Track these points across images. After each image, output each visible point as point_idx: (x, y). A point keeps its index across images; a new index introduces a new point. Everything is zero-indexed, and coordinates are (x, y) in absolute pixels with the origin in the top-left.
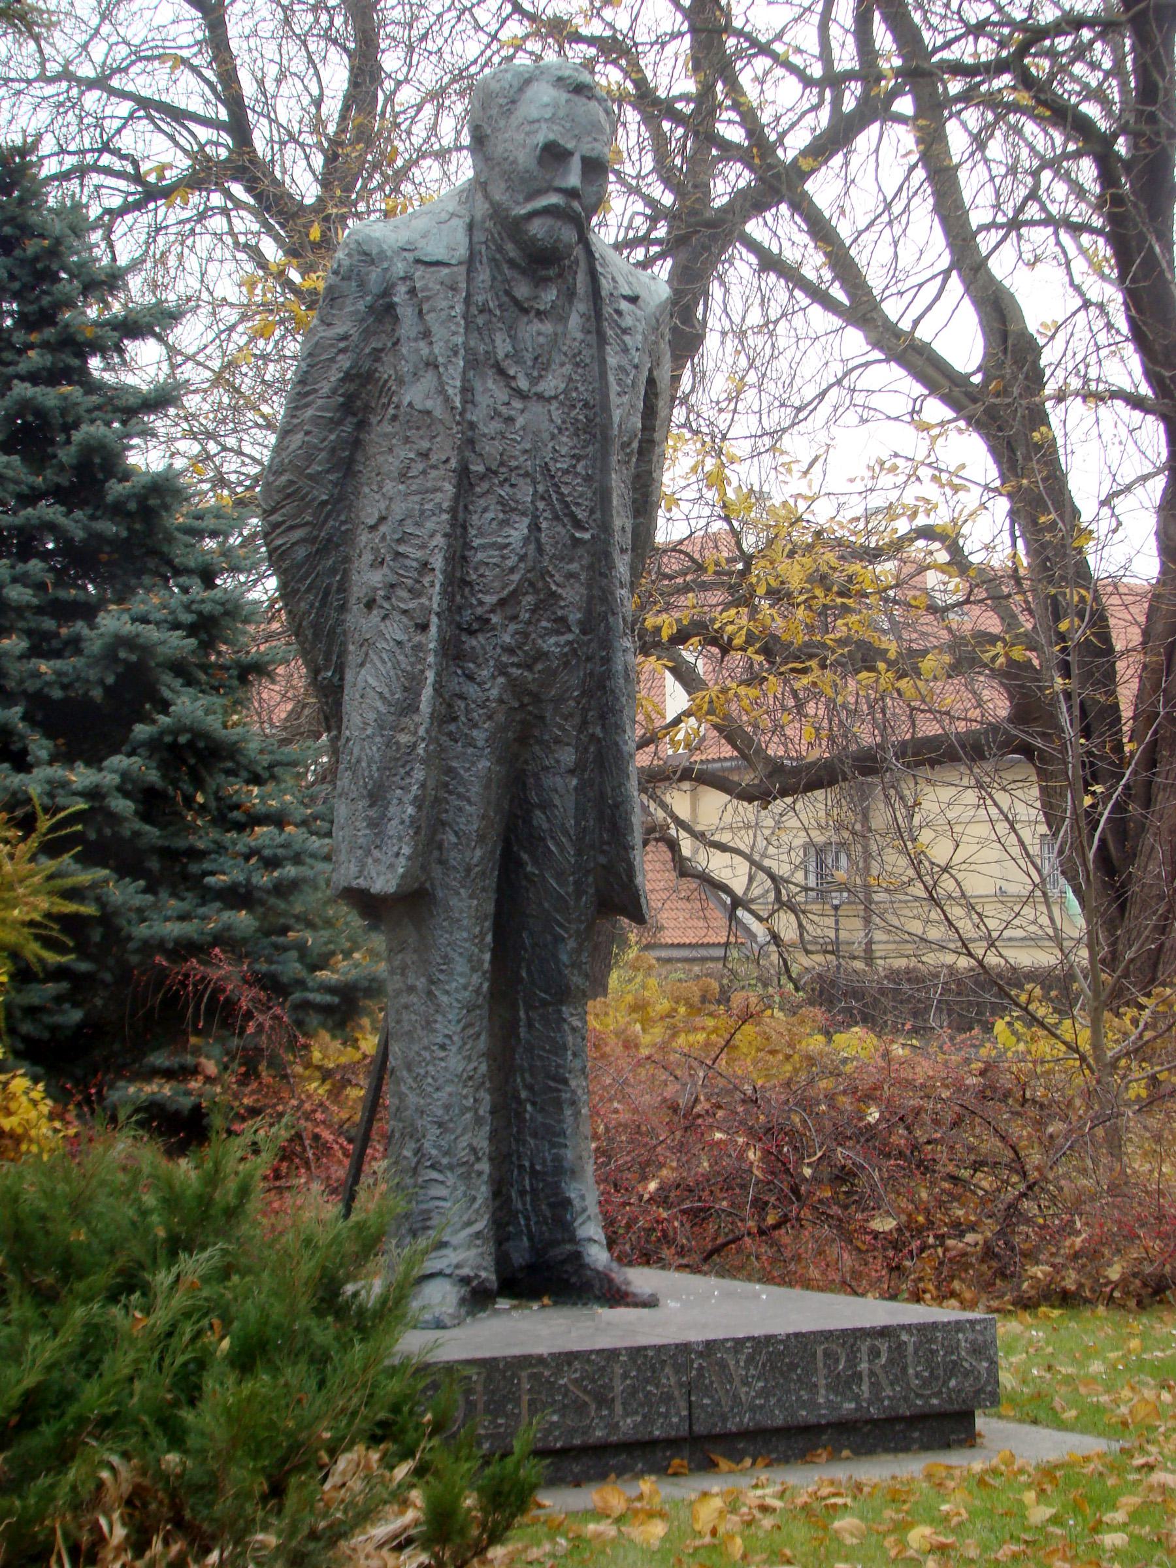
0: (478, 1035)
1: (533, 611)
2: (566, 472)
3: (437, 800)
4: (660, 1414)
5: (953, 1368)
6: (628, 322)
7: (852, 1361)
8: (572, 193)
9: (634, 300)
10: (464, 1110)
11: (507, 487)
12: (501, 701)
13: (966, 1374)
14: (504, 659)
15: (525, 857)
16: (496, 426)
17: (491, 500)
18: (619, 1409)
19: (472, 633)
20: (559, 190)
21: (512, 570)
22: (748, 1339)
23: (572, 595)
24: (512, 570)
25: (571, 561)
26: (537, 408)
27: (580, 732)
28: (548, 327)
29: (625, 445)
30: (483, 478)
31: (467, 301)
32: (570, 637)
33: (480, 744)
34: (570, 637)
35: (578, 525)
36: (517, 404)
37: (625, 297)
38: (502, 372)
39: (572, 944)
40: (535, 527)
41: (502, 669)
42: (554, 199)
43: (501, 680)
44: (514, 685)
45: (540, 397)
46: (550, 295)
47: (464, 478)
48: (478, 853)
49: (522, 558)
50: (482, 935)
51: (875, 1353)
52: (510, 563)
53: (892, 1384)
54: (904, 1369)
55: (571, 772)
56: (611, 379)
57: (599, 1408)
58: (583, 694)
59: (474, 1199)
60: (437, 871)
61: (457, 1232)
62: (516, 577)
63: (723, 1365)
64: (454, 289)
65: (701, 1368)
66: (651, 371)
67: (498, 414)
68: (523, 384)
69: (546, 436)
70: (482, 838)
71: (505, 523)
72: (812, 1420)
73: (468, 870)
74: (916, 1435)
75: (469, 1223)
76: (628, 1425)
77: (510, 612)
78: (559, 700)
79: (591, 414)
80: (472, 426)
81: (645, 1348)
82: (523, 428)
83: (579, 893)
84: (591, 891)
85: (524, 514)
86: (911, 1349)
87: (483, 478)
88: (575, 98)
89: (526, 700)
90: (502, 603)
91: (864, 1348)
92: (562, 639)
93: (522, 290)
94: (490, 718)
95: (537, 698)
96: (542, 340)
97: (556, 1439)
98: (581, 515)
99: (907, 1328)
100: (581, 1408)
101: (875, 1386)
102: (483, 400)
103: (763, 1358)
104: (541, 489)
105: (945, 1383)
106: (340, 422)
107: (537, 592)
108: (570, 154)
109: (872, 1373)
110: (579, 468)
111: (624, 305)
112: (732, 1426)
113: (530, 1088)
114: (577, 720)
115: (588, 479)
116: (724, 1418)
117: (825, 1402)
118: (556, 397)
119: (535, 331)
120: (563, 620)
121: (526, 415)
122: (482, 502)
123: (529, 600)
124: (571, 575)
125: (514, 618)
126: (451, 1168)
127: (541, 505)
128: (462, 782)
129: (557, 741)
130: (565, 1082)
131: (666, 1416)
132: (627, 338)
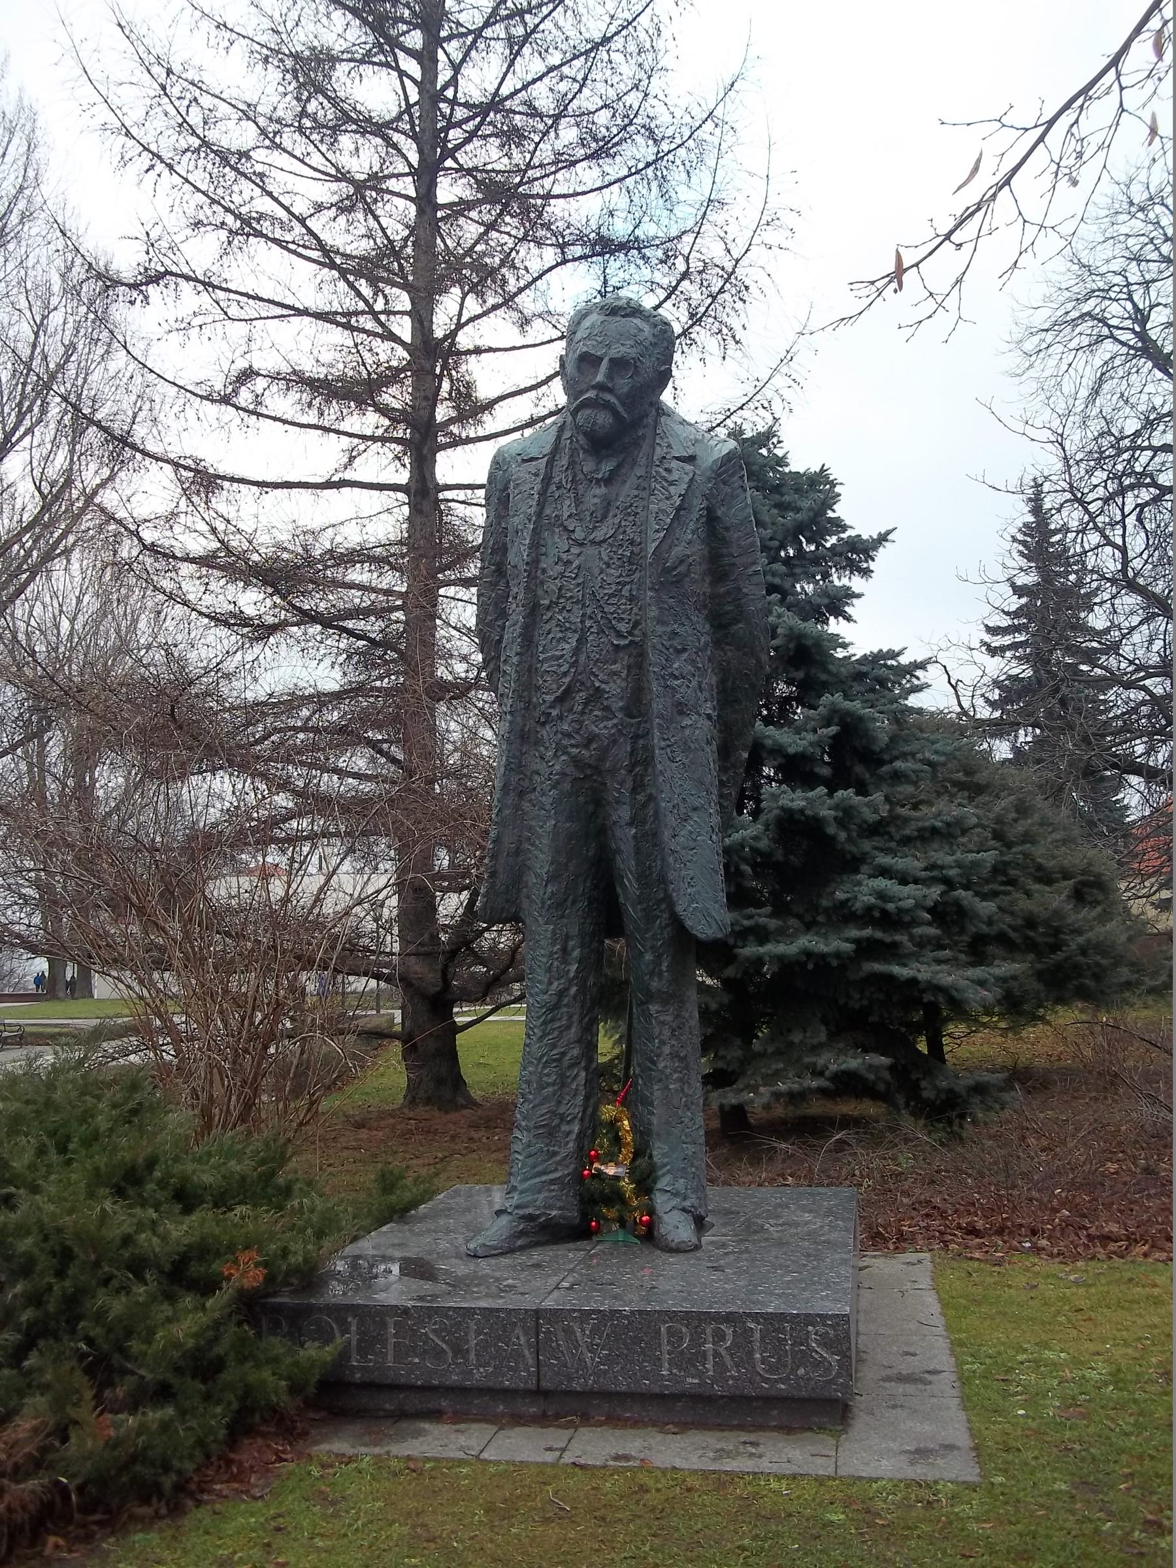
0: (569, 1027)
1: (586, 704)
2: (611, 596)
3: (518, 852)
4: (510, 1368)
5: (804, 1358)
6: (675, 476)
7: (697, 1340)
8: (601, 387)
9: (691, 459)
10: (541, 1087)
11: (565, 614)
12: (563, 774)
13: (817, 1365)
14: (565, 742)
15: (619, 890)
16: (560, 568)
17: (554, 622)
18: (472, 1356)
19: (543, 724)
20: (594, 387)
21: (565, 674)
22: (593, 1311)
23: (614, 688)
24: (565, 674)
25: (615, 663)
26: (591, 551)
27: (634, 791)
28: (601, 491)
29: (667, 571)
30: (549, 608)
31: (547, 480)
32: (615, 721)
33: (548, 807)
34: (615, 721)
35: (619, 635)
36: (575, 550)
37: (677, 458)
38: (566, 529)
39: (648, 957)
40: (581, 641)
41: (560, 749)
42: (591, 394)
43: (563, 758)
44: (576, 762)
45: (593, 542)
46: (607, 467)
47: (533, 611)
48: (549, 890)
49: (572, 665)
50: (565, 951)
51: (719, 1336)
52: (564, 669)
53: (737, 1366)
54: (751, 1353)
55: (630, 824)
56: (652, 519)
57: (455, 1356)
58: (633, 765)
59: (555, 1154)
60: (525, 904)
61: (526, 1180)
62: (567, 680)
63: (569, 1331)
64: (536, 475)
65: (548, 1332)
66: (710, 510)
67: (559, 559)
68: (579, 535)
69: (596, 571)
70: (553, 878)
71: (563, 639)
72: (656, 1390)
73: (543, 903)
74: (775, 1412)
75: (544, 1173)
76: (480, 1376)
77: (567, 705)
78: (613, 771)
79: (636, 550)
80: (544, 571)
81: (498, 1310)
82: (579, 567)
83: (649, 918)
84: (666, 915)
85: (575, 631)
86: (757, 1335)
87: (549, 608)
88: (610, 318)
89: (589, 772)
90: (560, 700)
91: (708, 1331)
92: (610, 724)
93: (588, 466)
94: (553, 787)
95: (597, 770)
96: (596, 500)
97: (417, 1378)
98: (623, 627)
99: (755, 1317)
100: (439, 1354)
101: (720, 1366)
102: (552, 552)
103: (608, 1330)
104: (589, 611)
105: (794, 1370)
106: (497, 584)
107: (587, 689)
108: (600, 359)
109: (716, 1354)
110: (625, 592)
111: (675, 464)
112: (576, 1386)
113: (639, 1065)
114: (629, 784)
115: (632, 598)
116: (570, 1379)
117: (667, 1374)
118: (604, 541)
119: (594, 496)
120: (607, 709)
121: (581, 558)
122: (548, 627)
123: (581, 696)
124: (615, 673)
125: (571, 710)
126: (528, 1129)
127: (588, 623)
128: (539, 837)
129: (618, 802)
130: (654, 1063)
131: (515, 1370)
132: (672, 489)
